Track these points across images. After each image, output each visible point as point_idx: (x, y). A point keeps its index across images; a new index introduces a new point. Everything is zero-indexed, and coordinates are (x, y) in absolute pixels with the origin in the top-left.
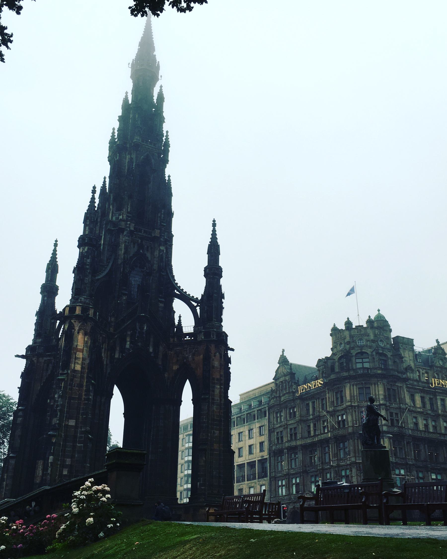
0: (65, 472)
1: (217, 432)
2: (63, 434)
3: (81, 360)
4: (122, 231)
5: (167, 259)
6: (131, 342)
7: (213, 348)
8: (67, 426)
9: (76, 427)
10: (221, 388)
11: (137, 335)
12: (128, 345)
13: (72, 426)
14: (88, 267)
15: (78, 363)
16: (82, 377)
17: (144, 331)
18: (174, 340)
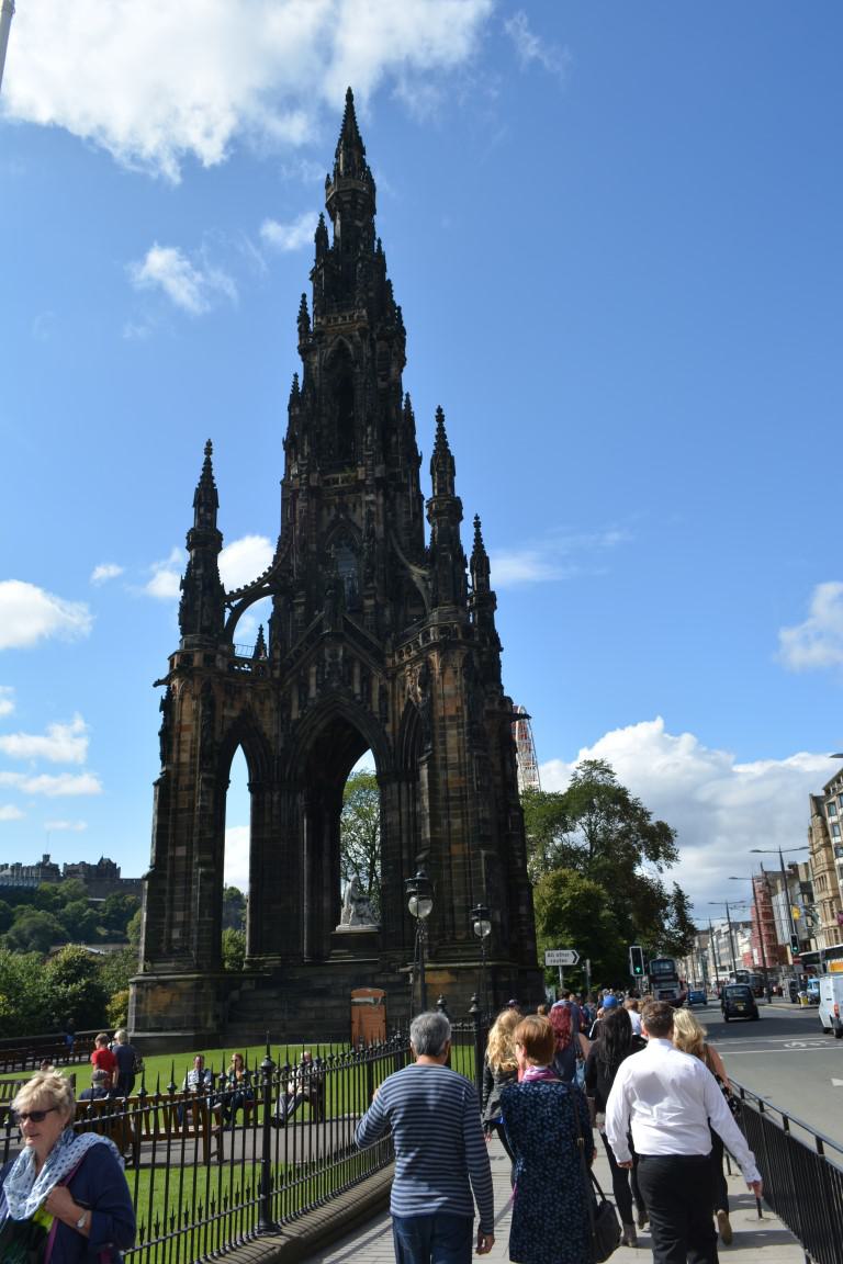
0: (176, 935)
1: (457, 823)
2: (168, 873)
3: (189, 743)
4: (296, 493)
5: (389, 514)
6: (318, 686)
7: (434, 657)
8: (172, 858)
9: (189, 857)
10: (459, 734)
11: (327, 669)
12: (313, 692)
13: (181, 857)
14: (198, 583)
15: (185, 751)
16: (193, 772)
17: (339, 659)
18: (394, 662)
